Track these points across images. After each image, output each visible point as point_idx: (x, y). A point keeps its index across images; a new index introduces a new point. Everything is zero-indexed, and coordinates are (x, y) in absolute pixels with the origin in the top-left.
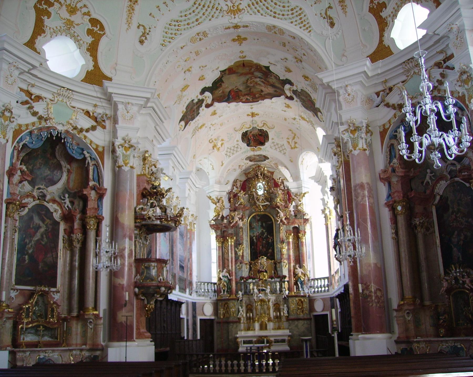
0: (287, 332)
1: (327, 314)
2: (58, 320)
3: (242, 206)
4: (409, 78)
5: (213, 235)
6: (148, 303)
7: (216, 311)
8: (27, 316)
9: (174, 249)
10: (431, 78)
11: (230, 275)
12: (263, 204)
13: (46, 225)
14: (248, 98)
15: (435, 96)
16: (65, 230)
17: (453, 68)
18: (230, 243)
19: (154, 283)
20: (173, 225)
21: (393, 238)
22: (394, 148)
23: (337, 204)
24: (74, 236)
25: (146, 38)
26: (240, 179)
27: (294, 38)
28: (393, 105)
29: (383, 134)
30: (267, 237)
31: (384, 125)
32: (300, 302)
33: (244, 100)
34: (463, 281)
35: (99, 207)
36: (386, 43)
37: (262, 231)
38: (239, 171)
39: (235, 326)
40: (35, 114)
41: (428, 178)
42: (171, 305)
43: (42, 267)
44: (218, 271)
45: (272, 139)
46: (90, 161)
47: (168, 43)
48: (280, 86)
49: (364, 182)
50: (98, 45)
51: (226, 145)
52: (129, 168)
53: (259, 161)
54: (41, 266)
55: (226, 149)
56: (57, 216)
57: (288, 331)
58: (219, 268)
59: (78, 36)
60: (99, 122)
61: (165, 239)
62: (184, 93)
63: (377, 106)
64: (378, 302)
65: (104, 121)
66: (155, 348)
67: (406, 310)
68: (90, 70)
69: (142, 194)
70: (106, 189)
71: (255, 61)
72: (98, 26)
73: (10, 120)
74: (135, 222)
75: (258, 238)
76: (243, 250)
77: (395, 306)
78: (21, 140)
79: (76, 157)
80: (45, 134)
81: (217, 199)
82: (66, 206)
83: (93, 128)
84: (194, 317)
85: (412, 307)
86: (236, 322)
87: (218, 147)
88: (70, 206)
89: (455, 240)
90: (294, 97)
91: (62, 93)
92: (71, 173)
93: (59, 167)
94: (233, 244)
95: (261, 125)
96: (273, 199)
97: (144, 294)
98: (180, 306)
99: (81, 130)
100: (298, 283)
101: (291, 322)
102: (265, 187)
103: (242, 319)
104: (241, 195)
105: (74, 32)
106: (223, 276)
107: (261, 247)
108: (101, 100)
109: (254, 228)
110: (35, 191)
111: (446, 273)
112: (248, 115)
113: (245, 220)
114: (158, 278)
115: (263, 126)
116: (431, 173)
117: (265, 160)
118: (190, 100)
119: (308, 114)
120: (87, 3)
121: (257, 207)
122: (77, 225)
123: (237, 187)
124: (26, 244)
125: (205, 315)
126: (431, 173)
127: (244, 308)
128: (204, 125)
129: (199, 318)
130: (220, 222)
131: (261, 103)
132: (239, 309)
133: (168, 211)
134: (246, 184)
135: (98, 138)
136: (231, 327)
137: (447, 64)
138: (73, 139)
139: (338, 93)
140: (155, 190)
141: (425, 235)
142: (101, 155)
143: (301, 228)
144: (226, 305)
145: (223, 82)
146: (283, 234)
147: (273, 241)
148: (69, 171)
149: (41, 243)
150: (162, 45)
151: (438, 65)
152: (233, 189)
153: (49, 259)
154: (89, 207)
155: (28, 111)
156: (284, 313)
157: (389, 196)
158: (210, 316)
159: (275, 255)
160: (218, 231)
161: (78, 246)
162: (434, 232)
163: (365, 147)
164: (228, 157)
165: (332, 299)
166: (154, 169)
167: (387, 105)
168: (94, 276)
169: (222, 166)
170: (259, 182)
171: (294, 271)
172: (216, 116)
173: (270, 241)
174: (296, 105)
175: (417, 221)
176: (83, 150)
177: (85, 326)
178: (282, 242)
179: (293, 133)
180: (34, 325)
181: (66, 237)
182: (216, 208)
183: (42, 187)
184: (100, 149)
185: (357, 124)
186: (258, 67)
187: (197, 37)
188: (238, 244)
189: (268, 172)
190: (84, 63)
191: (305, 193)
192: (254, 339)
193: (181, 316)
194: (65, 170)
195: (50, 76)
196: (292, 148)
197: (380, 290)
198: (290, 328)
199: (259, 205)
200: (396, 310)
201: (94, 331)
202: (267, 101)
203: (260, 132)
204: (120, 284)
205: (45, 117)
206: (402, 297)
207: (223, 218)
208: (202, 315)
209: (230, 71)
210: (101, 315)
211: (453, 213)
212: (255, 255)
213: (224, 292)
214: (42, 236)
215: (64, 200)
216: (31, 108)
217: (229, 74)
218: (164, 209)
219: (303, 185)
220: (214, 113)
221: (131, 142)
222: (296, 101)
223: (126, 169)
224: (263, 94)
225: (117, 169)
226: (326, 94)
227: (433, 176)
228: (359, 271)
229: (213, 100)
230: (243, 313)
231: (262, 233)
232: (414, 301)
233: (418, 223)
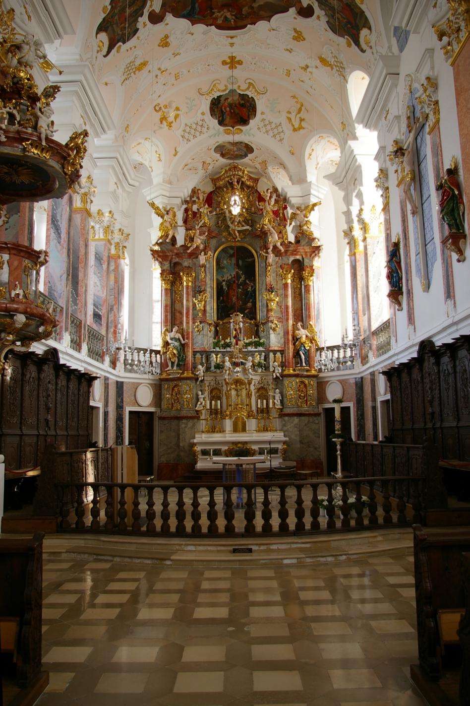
0: (279, 436)
1: (349, 408)
7: (158, 398)
12: (239, 229)
14: (228, 15)
18: (185, 283)
20: (57, 167)
30: (244, 283)
33: (220, 21)
37: (237, 273)
39: (190, 424)
42: (68, 380)
44: (163, 330)
45: (262, 113)
51: (184, 120)
55: (183, 125)
57: (282, 434)
58: (166, 326)
61: (59, 247)
75: (230, 284)
76: (205, 302)
81: (165, 210)
84: (120, 407)
86: (192, 418)
94: (190, 284)
96: (255, 222)
100: (301, 352)
101: (286, 418)
102: (243, 203)
103: (203, 412)
104: (205, 212)
106: (171, 339)
107: (234, 299)
109: (223, 268)
114: (10, 294)
115: (248, 88)
117: (246, 156)
121: (230, 234)
125: (139, 406)
127: (206, 393)
128: (144, 64)
129: (128, 409)
132: (197, 395)
136: (183, 426)
143: (306, 262)
144: (176, 389)
147: (254, 291)
156: (274, 404)
158: (148, 406)
159: (258, 312)
160: (165, 262)
164: (185, 140)
169: (175, 155)
171: (294, 332)
172: (168, 51)
178: (271, 290)
182: (162, 224)
189: (251, 178)
191: (315, 205)
192: (224, 448)
196: (295, 130)
198: (285, 428)
199: (234, 231)
203: (242, 100)
208: (133, 405)
212: (224, 310)
213: (172, 367)
230: (205, 402)
231: (238, 276)
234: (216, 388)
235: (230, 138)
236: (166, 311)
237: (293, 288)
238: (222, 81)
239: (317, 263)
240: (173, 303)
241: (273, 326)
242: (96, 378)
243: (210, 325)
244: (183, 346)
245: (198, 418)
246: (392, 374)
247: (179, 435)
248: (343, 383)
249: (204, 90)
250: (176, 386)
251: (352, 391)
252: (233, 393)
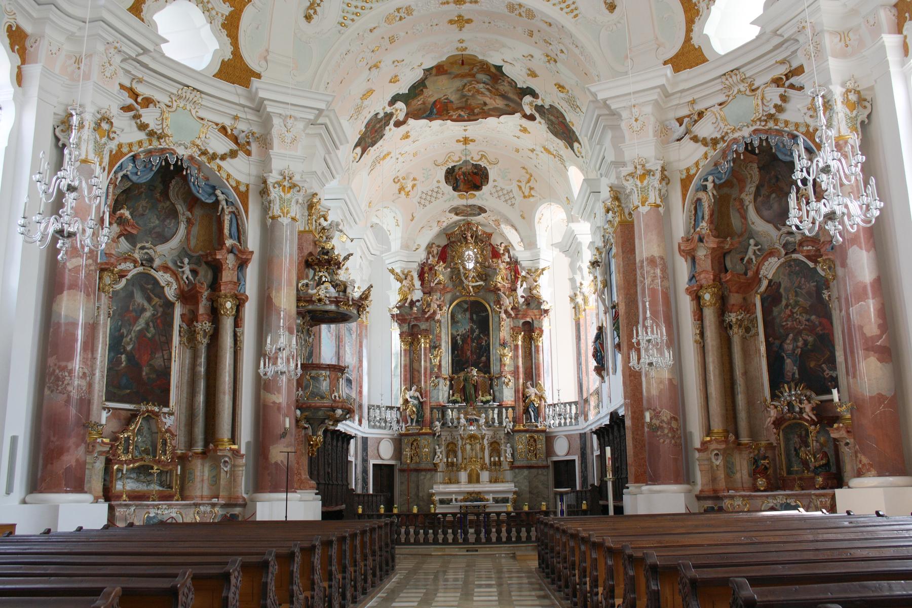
0: (510, 486)
2: (172, 458)
3: (441, 287)
4: (731, 98)
5: (395, 331)
6: (314, 433)
7: (398, 452)
8: (126, 451)
9: (341, 352)
10: (765, 101)
11: (421, 395)
13: (154, 306)
14: (462, 113)
15: (770, 129)
16: (182, 316)
17: (801, 88)
19: (327, 402)
20: (355, 312)
21: (696, 341)
22: (701, 205)
23: (604, 287)
24: (199, 326)
25: (315, 12)
26: (437, 243)
27: (550, 25)
28: (704, 139)
29: (685, 183)
31: (688, 170)
32: (532, 440)
33: (454, 117)
34: (801, 409)
35: (239, 281)
36: (696, 41)
37: (472, 327)
38: (436, 230)
39: (428, 476)
40: (142, 127)
41: (750, 254)
43: (147, 374)
44: (403, 389)
46: (225, 207)
47: (350, 22)
48: (516, 98)
49: (656, 254)
50: (239, 19)
51: (420, 188)
53: (471, 215)
54: (145, 371)
55: (420, 193)
56: (170, 293)
57: (513, 485)
58: (405, 385)
60: (240, 145)
62: (366, 102)
63: (678, 140)
64: (673, 437)
65: (248, 143)
66: (323, 505)
67: (713, 450)
68: (226, 60)
69: (307, 261)
70: (252, 252)
71: (480, 57)
73: (108, 136)
74: (298, 307)
75: (464, 338)
77: (697, 445)
78: (121, 167)
79: (203, 199)
80: (156, 161)
82: (185, 277)
83: (233, 154)
84: (365, 461)
85: (724, 446)
86: (430, 470)
87: (407, 190)
88: (190, 277)
89: (788, 346)
90: (537, 115)
91: (184, 95)
92: (193, 224)
93: (173, 214)
95: (476, 157)
97: (308, 420)
98: (348, 443)
99: (214, 157)
101: (517, 470)
102: (476, 258)
103: (441, 465)
107: (469, 353)
108: (246, 109)
109: (458, 322)
110: (137, 251)
111: (774, 396)
112: (458, 141)
113: (445, 308)
115: (481, 159)
116: (756, 245)
117: (479, 214)
118: (372, 114)
119: (558, 144)
121: (464, 288)
122: (203, 307)
123: (433, 256)
124: (122, 336)
126: (756, 245)
127: (443, 448)
129: (372, 462)
130: (408, 310)
131: (481, 123)
132: (435, 449)
133: (349, 290)
134: (447, 249)
135: (239, 170)
136: (422, 477)
137: (793, 80)
138: (199, 170)
139: (620, 116)
140: (326, 257)
141: (744, 339)
142: (244, 197)
143: (536, 324)
145: (425, 87)
146: (505, 333)
147: (489, 344)
148: (189, 221)
149: (145, 336)
150: (341, 24)
151: (777, 82)
152: (428, 259)
153: (158, 362)
154: (224, 279)
155: (133, 122)
157: (692, 278)
161: (203, 342)
162: (757, 334)
163: (658, 202)
165: (583, 436)
166: (325, 224)
167: (695, 139)
168: (232, 390)
170: (468, 249)
171: (524, 390)
173: (484, 343)
174: (539, 129)
175: (733, 317)
176: (214, 188)
177: (216, 467)
178: (503, 345)
179: (527, 173)
180: (136, 465)
181: (184, 326)
182: (401, 289)
183: (148, 245)
184: (242, 188)
185: (648, 166)
186: (485, 67)
187: (396, 13)
188: (435, 347)
189: (484, 233)
190: (218, 47)
191: (543, 270)
193: (349, 459)
194: (182, 218)
195: (168, 67)
196: (525, 197)
197: (676, 420)
200: (699, 450)
201: (231, 475)
202: (492, 121)
204: (274, 403)
205: (159, 132)
206: (709, 432)
207: (412, 303)
208: (376, 459)
209: (439, 70)
210: (243, 451)
211: (787, 306)
212: (459, 364)
214: (147, 324)
215: (182, 267)
216: (137, 117)
217: (436, 75)
218: (342, 287)
219: (542, 256)
220: (406, 136)
221: (294, 179)
222: (540, 123)
223: (285, 221)
224: (486, 108)
226: (599, 116)
227: (759, 250)
228: (644, 390)
229: (408, 116)
230: (441, 458)
231: (472, 331)
232: (726, 437)
233: (734, 320)
234: (452, 443)
235: (463, 202)
236: (405, 371)
237: (524, 347)
238: (457, 156)
239: (546, 323)
240: (411, 362)
241: (506, 380)
242: (352, 437)
243: (445, 379)
244: (421, 403)
245: (436, 470)
246: (601, 432)
247: (418, 487)
248: (569, 437)
249: (440, 161)
250: (415, 440)
251: (577, 444)
252: (468, 447)
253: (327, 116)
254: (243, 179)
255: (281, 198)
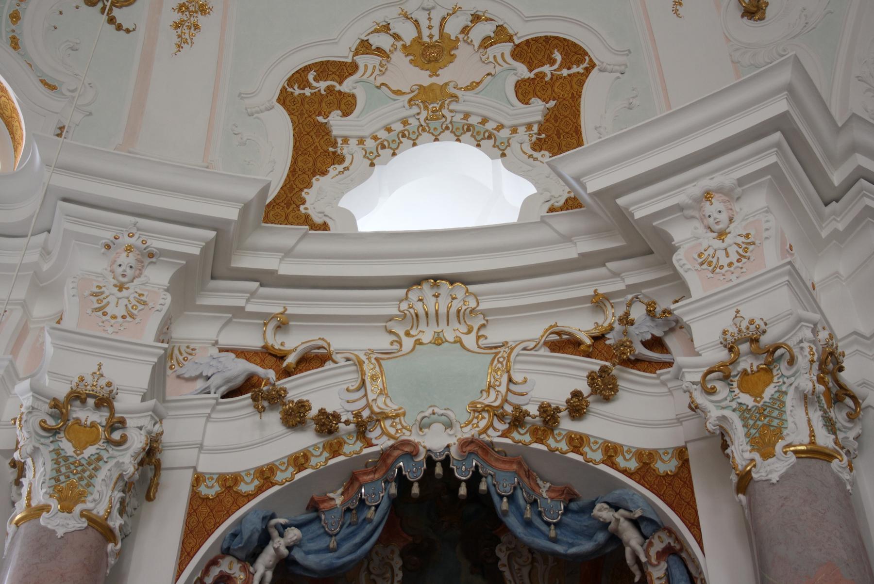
40: (295, 417)
52: (793, 459)
59: (485, 121)
60: (622, 355)
72: (558, 56)
79: (559, 549)
80: (379, 493)
83: (604, 387)
91: (419, 307)
99: (549, 415)
105: (467, 115)
108: (610, 265)
120: (480, 7)
142: (678, 488)
184: (666, 466)
223: (772, 469)
225: (741, 496)
253: (854, 148)
254: (660, 440)
255: (743, 411)
